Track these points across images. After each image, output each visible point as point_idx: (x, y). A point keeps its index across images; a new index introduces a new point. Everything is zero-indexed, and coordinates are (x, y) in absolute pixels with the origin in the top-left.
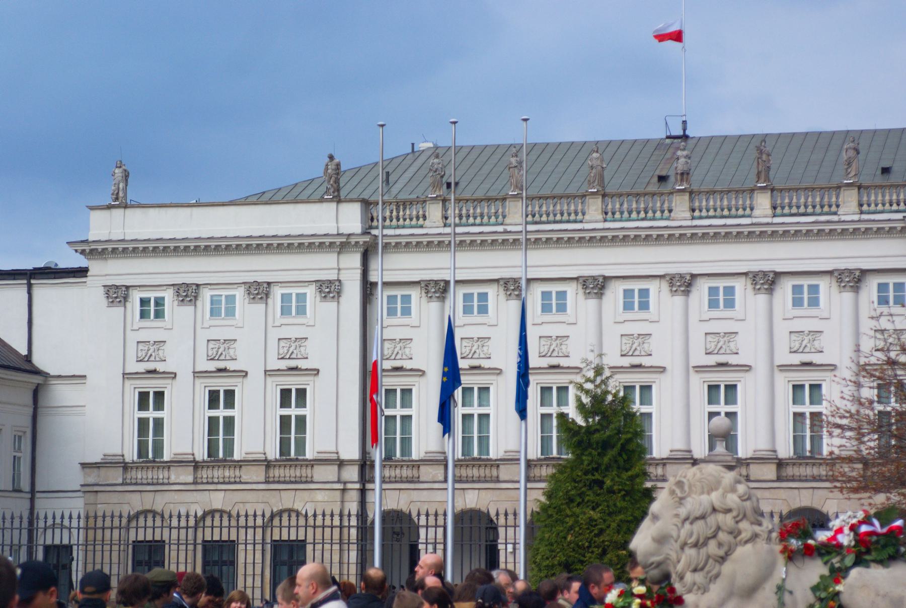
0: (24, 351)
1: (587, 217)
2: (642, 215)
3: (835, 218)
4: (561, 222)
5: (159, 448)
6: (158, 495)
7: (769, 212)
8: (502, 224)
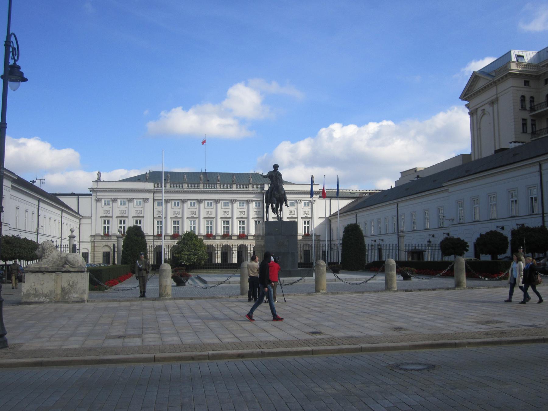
0: (76, 211)
1: (200, 188)
2: (211, 188)
3: (248, 190)
4: (194, 188)
5: (108, 232)
6: (109, 242)
7: (236, 188)
8: (182, 188)
